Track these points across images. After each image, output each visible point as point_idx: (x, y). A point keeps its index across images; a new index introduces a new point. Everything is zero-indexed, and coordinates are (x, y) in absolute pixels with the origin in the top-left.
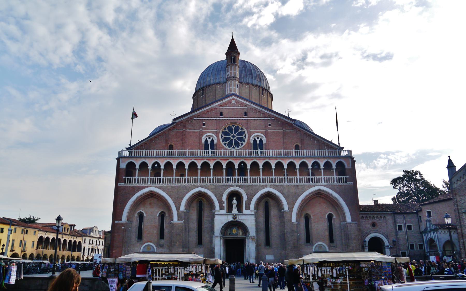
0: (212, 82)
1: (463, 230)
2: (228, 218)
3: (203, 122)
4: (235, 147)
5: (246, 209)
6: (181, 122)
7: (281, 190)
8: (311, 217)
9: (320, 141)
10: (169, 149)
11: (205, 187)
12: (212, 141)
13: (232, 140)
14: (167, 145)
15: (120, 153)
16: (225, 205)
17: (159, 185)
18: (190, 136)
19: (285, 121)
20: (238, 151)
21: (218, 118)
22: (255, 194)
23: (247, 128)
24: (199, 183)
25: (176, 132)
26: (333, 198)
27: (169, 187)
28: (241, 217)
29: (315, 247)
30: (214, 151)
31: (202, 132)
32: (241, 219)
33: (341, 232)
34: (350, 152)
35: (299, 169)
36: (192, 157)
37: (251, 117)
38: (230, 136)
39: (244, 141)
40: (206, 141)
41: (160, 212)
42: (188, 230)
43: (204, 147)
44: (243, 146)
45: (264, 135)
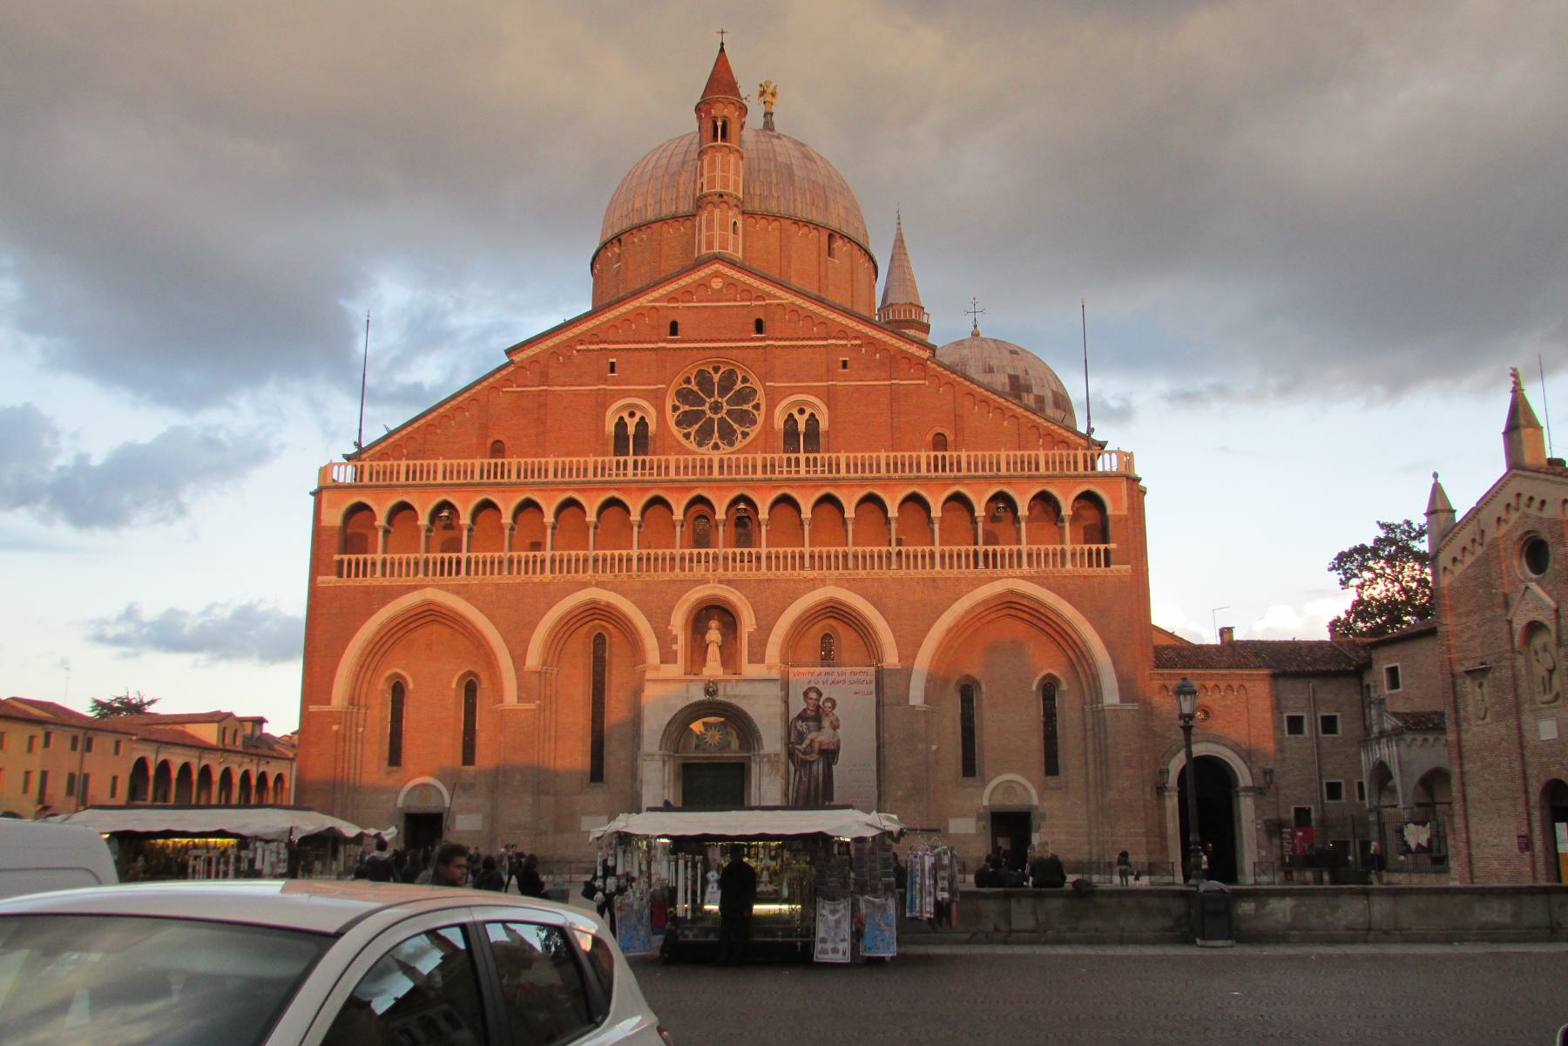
0: (650, 216)
1: (1463, 734)
2: (687, 690)
4: (720, 444)
5: (750, 662)
6: (534, 360)
8: (980, 688)
9: (1021, 421)
10: (491, 457)
11: (610, 586)
12: (643, 423)
13: (712, 420)
14: (485, 444)
15: (325, 471)
16: (680, 646)
17: (454, 580)
19: (899, 348)
20: (725, 457)
23: (763, 378)
24: (590, 572)
25: (516, 394)
26: (1060, 622)
27: (487, 588)
29: (993, 791)
30: (644, 462)
32: (735, 696)
33: (1085, 738)
34: (1127, 459)
35: (942, 520)
36: (565, 483)
38: (704, 408)
39: (754, 422)
40: (621, 425)
41: (460, 673)
42: (553, 733)
43: (611, 447)
44: (749, 439)
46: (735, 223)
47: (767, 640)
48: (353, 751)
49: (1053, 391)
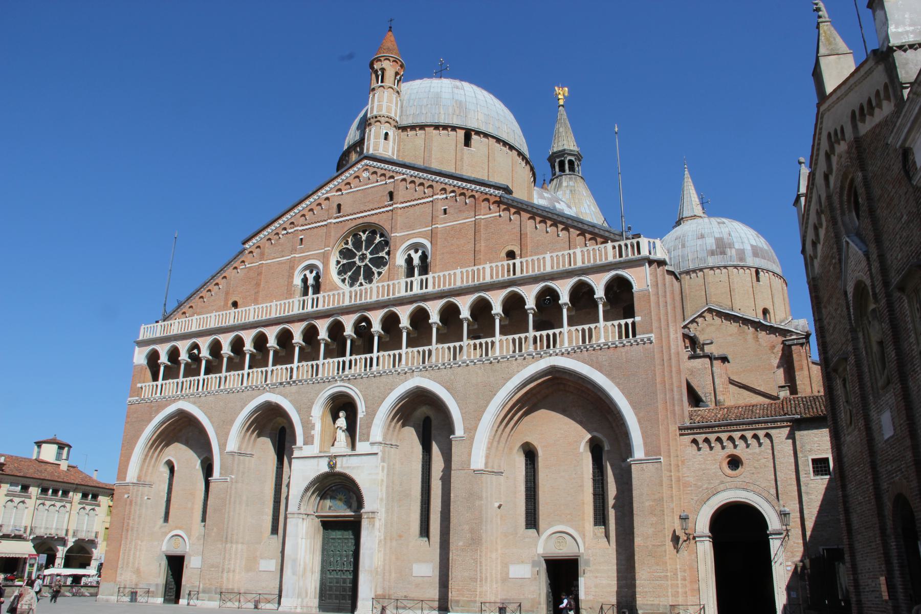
2: (318, 465)
3: (298, 236)
4: (364, 283)
13: (360, 267)
21: (329, 221)
22: (384, 399)
32: (348, 467)
37: (403, 201)
38: (355, 260)
41: (202, 458)
45: (428, 240)
46: (387, 134)
47: (372, 423)
48: (138, 512)
49: (752, 246)
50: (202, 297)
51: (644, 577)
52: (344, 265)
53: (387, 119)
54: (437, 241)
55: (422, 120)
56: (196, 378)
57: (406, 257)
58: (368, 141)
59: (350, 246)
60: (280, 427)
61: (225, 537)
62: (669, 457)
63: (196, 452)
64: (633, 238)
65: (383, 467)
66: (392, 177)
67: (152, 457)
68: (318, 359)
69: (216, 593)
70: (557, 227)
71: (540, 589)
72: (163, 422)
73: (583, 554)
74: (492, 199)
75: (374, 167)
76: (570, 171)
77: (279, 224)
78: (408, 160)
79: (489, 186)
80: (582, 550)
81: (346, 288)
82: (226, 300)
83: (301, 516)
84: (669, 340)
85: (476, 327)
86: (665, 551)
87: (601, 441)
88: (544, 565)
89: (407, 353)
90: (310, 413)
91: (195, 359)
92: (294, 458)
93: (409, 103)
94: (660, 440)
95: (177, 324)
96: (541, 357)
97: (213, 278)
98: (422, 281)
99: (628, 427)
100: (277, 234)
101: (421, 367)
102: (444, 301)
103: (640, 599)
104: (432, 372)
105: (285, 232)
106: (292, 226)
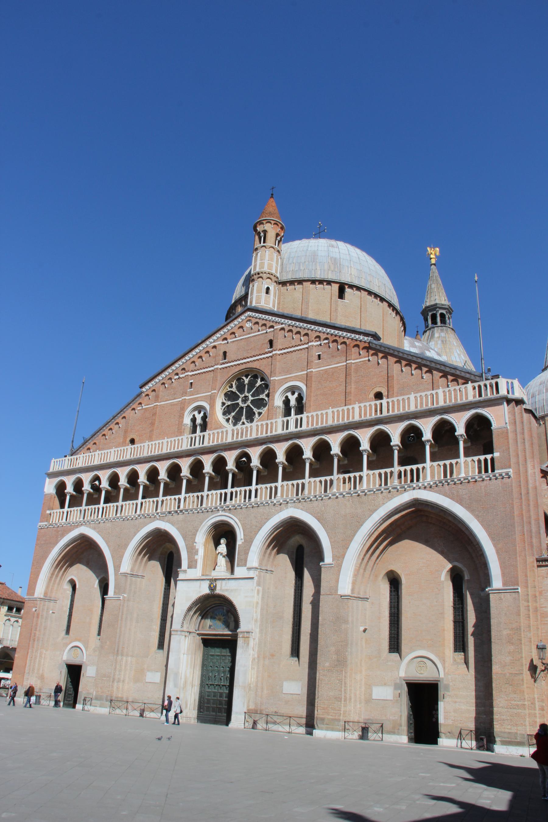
2: (200, 587)
3: (188, 381)
4: (246, 422)
7: (318, 513)
13: (242, 408)
18: (166, 413)
21: (216, 367)
22: (261, 528)
25: (143, 410)
28: (226, 583)
31: (185, 402)
32: (227, 590)
37: (281, 348)
38: (238, 401)
41: (100, 578)
46: (268, 289)
47: (249, 550)
50: (104, 435)
51: (502, 705)
52: (228, 406)
53: (268, 276)
54: (311, 384)
55: (300, 276)
56: (97, 506)
57: (284, 398)
58: (251, 295)
59: (234, 389)
60: (168, 552)
61: (116, 650)
62: (527, 587)
63: (95, 572)
64: (492, 379)
65: (258, 591)
66: (272, 327)
67: (57, 576)
68: (203, 491)
69: (107, 701)
70: (421, 370)
71: (401, 712)
72: (67, 545)
73: (443, 678)
74: (362, 345)
75: (256, 318)
76: (441, 323)
77: (172, 369)
78: (286, 312)
79: (359, 333)
80: (442, 675)
81: (229, 427)
82: (125, 437)
83: (183, 633)
84: (527, 475)
85: (346, 462)
86: (523, 680)
87: (462, 571)
88: (406, 688)
89: (282, 486)
90: (195, 540)
91: (97, 489)
92: (179, 580)
93: (289, 261)
94: (517, 571)
95: (81, 458)
96: (405, 490)
97: (114, 417)
98: (297, 420)
99: (487, 557)
100: (170, 379)
101: (295, 499)
102: (317, 438)
103: (497, 726)
104: (305, 503)
105: (177, 377)
106: (184, 371)
